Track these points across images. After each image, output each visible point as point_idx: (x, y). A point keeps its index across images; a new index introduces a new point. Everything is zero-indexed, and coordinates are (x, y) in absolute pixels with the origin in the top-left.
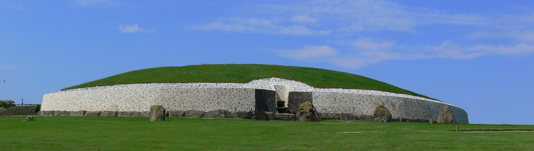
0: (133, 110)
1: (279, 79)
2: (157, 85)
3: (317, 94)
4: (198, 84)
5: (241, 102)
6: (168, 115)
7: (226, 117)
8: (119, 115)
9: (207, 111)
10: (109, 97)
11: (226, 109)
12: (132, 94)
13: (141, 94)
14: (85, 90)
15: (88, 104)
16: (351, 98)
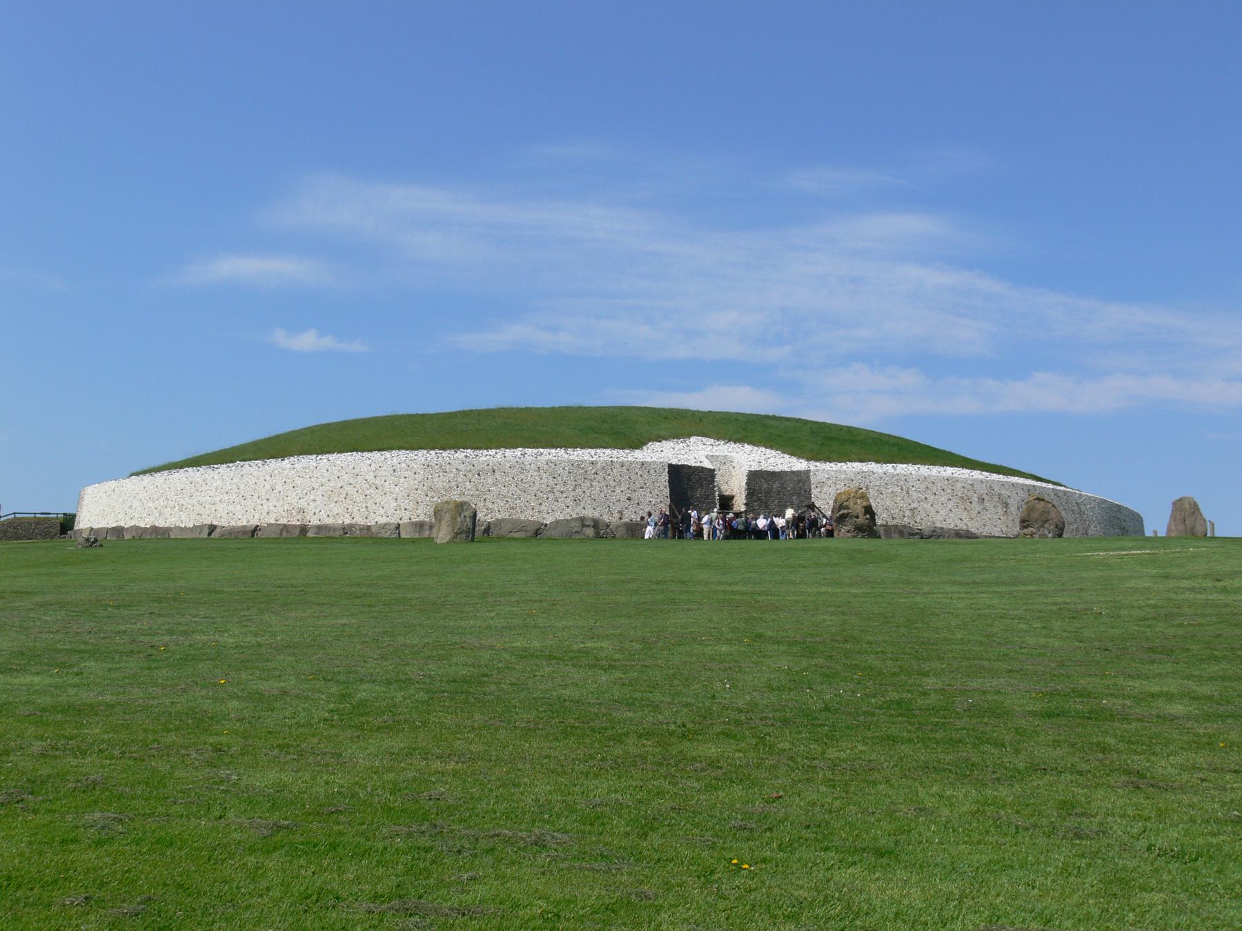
0: (347, 521)
1: (711, 441)
2: (411, 454)
3: (821, 476)
4: (518, 452)
5: (633, 496)
6: (480, 529)
7: (598, 536)
8: (310, 535)
9: (549, 520)
10: (279, 488)
11: (596, 515)
12: (346, 477)
13: (370, 477)
14: (210, 471)
15: (220, 507)
16: (904, 484)
